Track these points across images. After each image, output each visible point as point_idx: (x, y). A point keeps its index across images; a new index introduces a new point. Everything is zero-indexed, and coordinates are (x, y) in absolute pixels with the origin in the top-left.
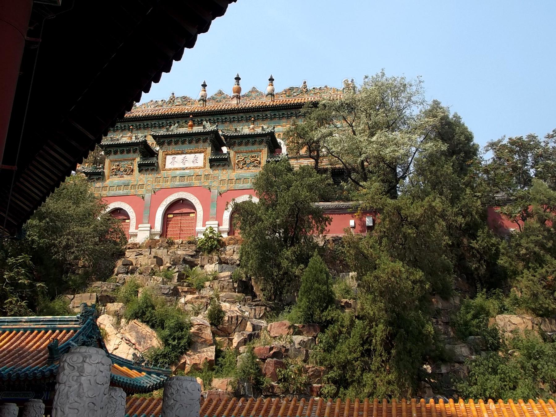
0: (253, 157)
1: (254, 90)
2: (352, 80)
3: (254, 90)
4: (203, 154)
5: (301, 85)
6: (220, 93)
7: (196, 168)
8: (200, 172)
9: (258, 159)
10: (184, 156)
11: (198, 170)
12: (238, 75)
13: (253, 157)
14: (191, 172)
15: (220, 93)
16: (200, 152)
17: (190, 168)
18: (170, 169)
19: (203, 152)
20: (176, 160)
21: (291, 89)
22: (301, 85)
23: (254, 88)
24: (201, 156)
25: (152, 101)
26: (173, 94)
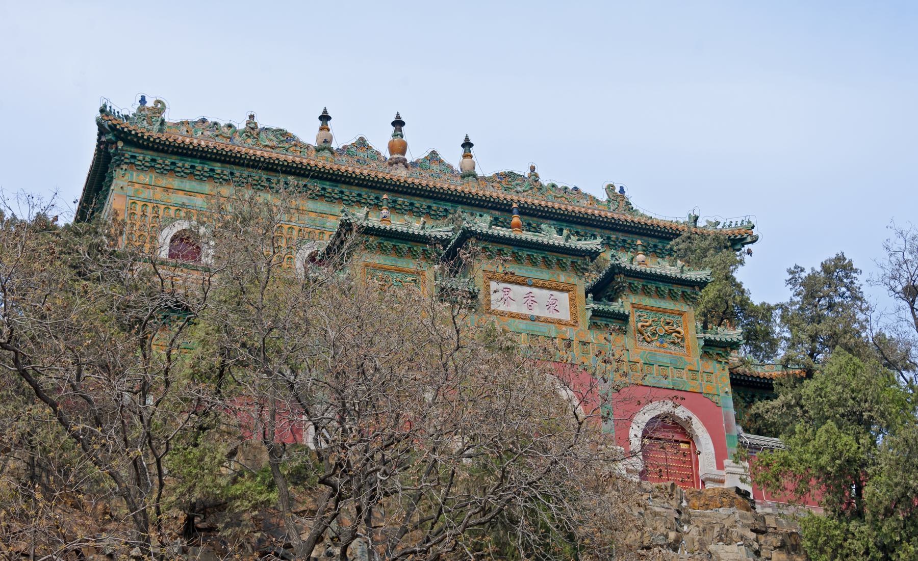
0: (668, 323)
1: (434, 156)
2: (622, 188)
3: (434, 156)
4: (565, 296)
5: (526, 172)
6: (362, 143)
7: (559, 322)
8: (570, 333)
9: (678, 329)
10: (527, 289)
11: (564, 328)
12: (398, 116)
13: (668, 323)
14: (552, 331)
15: (362, 143)
16: (562, 290)
17: (547, 321)
18: (502, 314)
19: (568, 291)
20: (511, 294)
21: (510, 175)
22: (526, 172)
23: (433, 152)
24: (564, 298)
25: (204, 121)
26: (252, 117)
